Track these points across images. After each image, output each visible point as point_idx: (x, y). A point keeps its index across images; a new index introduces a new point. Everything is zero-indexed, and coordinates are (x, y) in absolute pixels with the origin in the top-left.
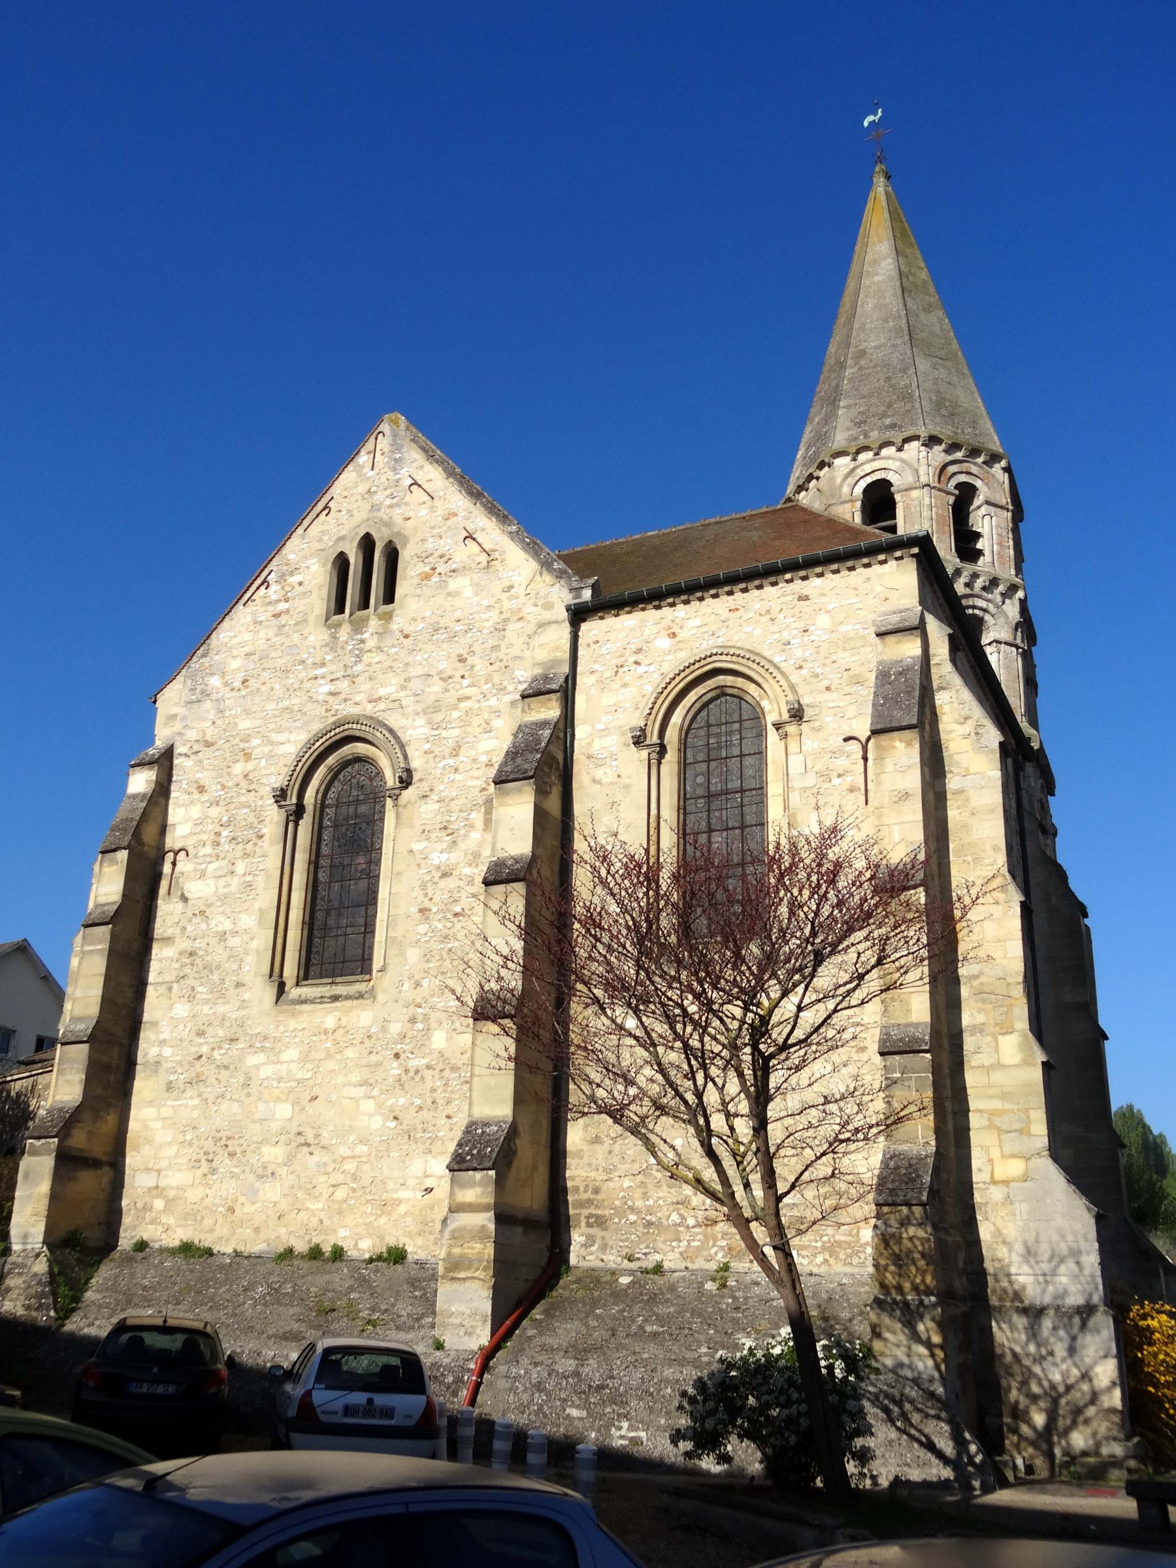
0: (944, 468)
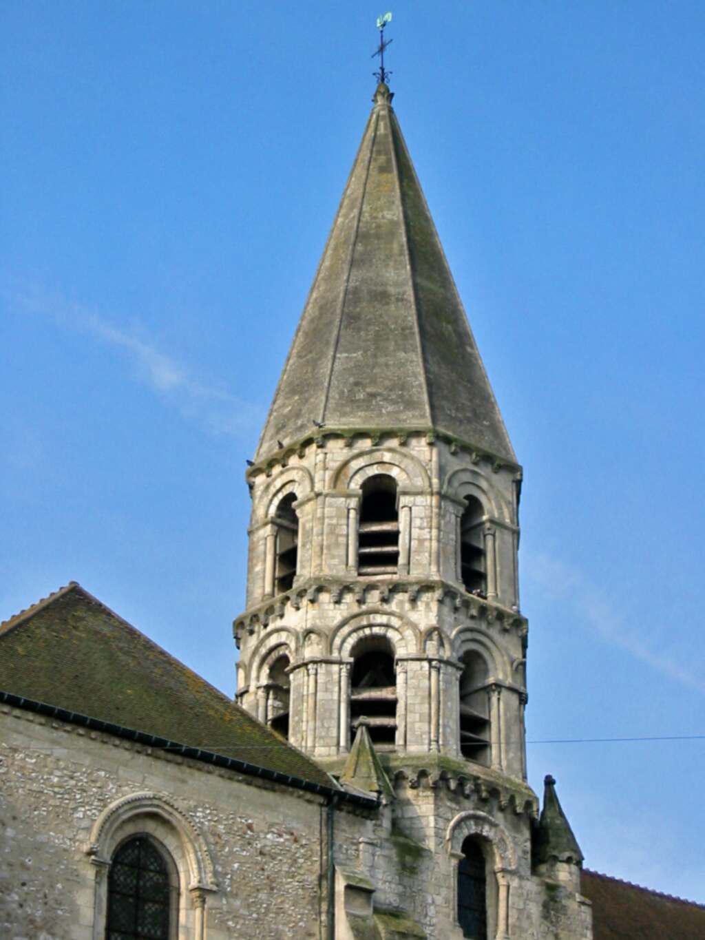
0: (346, 464)
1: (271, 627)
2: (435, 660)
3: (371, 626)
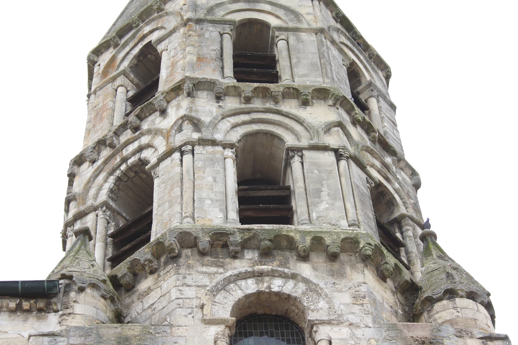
3: (124, 160)
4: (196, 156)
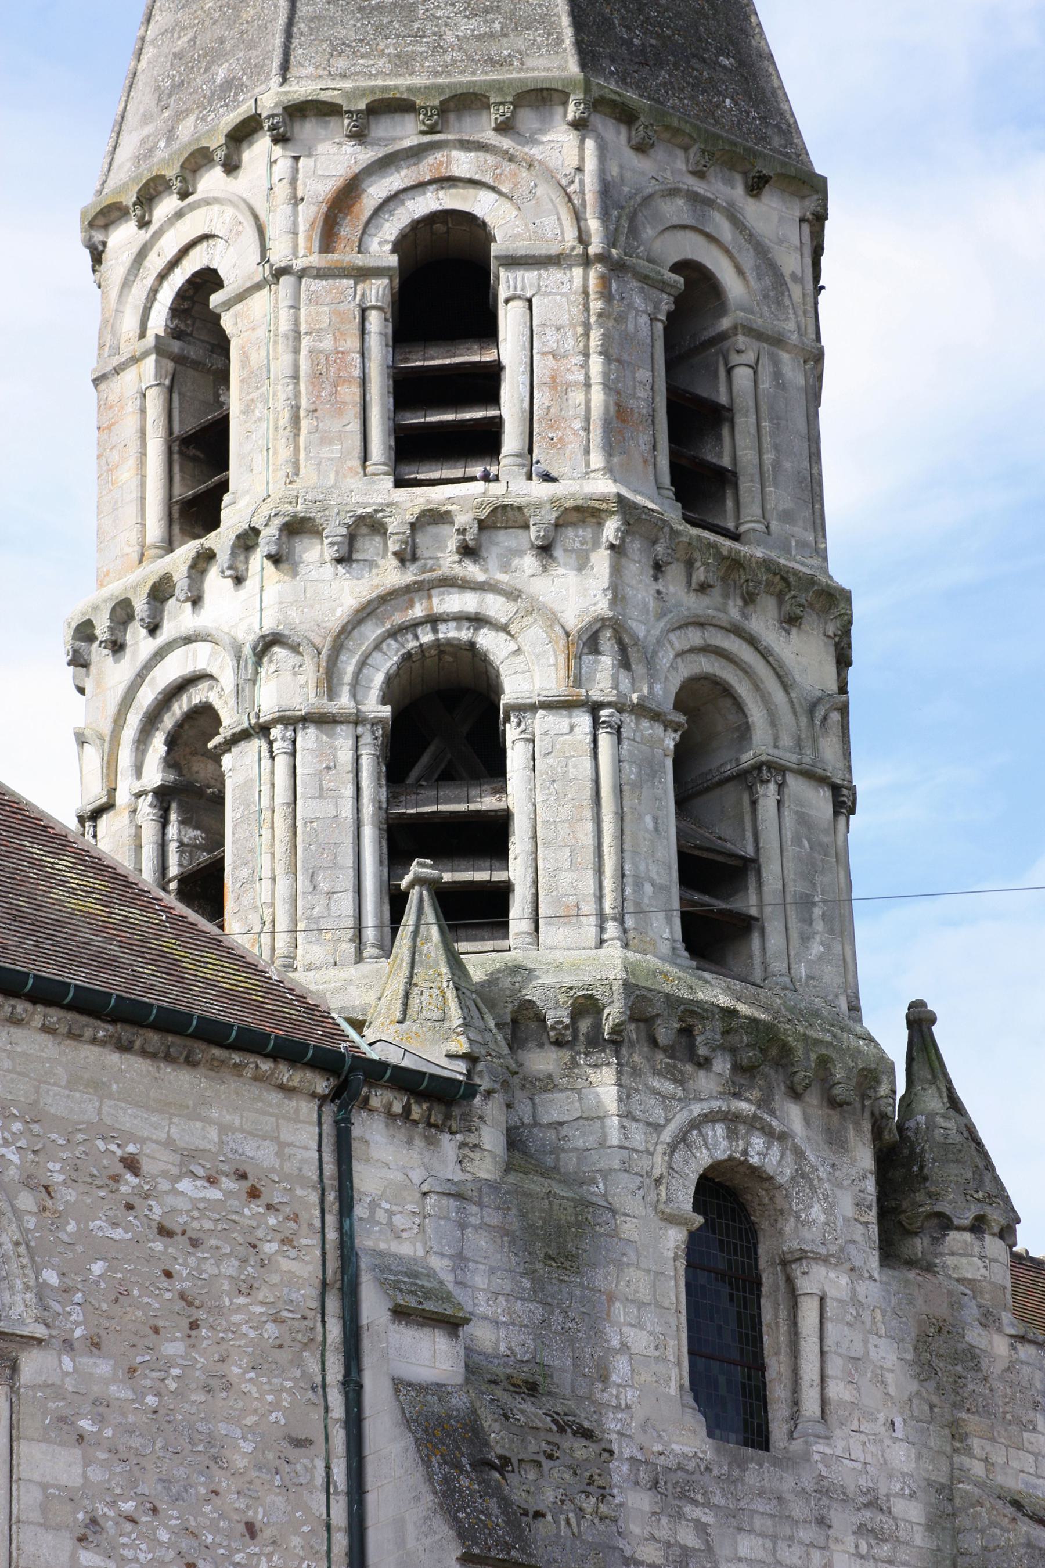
1: (168, 631)
2: (609, 705)
3: (433, 621)
4: (625, 745)
